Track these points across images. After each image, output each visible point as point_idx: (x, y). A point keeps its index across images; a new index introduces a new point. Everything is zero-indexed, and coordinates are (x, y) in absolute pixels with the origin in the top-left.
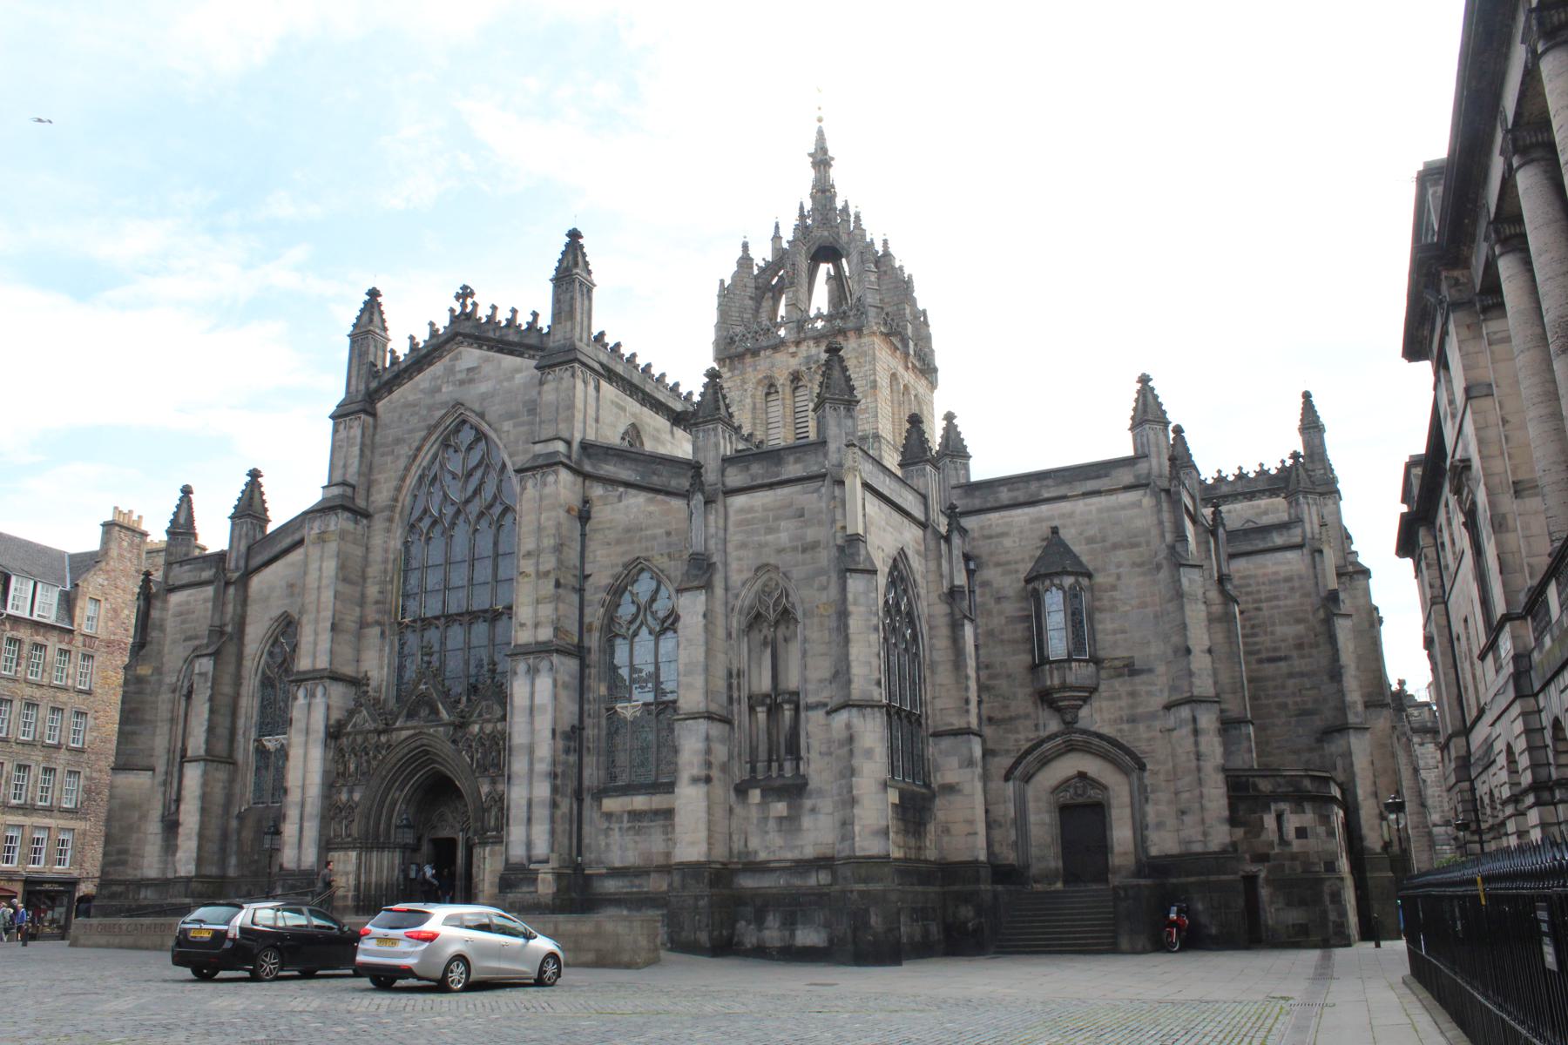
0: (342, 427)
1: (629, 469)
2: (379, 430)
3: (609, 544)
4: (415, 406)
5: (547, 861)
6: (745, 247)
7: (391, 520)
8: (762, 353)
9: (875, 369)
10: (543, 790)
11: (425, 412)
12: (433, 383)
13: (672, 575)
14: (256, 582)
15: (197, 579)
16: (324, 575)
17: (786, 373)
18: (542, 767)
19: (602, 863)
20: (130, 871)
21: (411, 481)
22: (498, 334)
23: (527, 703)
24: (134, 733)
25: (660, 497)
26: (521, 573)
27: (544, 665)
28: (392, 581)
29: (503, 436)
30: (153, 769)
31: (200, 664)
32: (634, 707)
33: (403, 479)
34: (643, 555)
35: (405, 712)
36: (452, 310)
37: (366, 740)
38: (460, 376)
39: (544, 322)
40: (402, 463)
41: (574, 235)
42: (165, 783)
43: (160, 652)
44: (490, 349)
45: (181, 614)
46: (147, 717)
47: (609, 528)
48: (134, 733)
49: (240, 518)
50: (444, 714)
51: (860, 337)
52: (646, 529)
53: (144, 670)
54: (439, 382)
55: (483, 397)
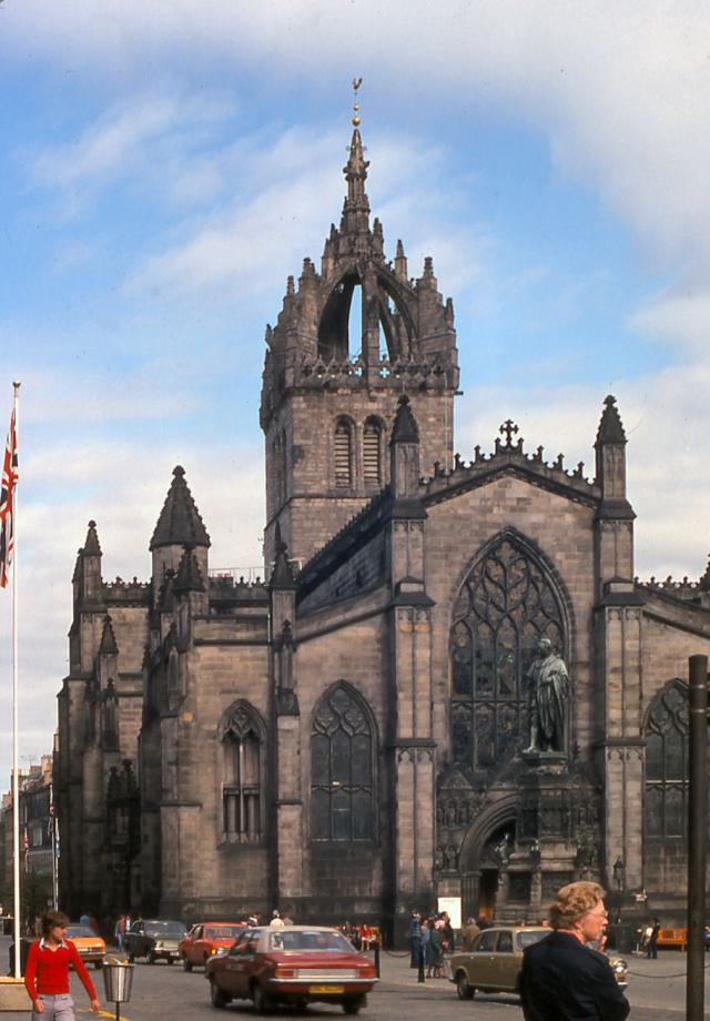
0: (401, 527)
4: (467, 519)
11: (477, 528)
14: (304, 651)
16: (419, 661)
22: (548, 475)
24: (187, 773)
29: (556, 564)
36: (498, 441)
38: (509, 503)
42: (216, 817)
43: (195, 701)
44: (539, 486)
45: (212, 668)
46: (193, 759)
48: (187, 773)
53: (188, 717)
54: (489, 503)
55: (535, 527)
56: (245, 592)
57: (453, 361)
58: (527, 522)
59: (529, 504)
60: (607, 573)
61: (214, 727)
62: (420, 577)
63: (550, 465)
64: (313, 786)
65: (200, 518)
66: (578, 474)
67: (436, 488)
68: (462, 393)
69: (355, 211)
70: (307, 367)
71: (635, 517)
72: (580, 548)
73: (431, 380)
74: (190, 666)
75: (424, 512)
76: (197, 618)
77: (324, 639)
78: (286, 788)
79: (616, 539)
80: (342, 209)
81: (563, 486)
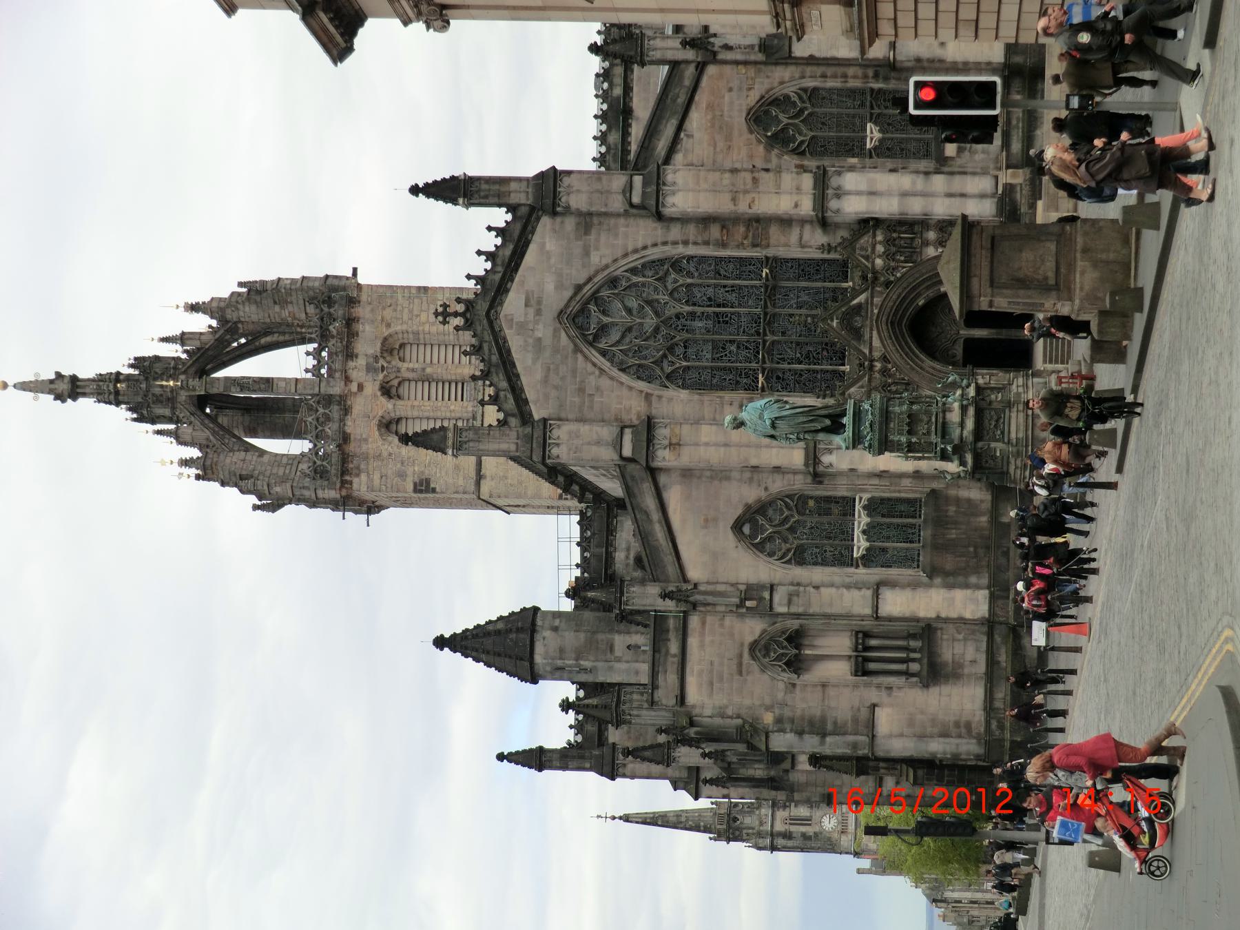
1: (666, 126)
2: (563, 415)
3: (730, 147)
4: (549, 369)
5: (996, 178)
6: (185, 463)
7: (660, 397)
8: (348, 430)
9: (403, 288)
10: (939, 182)
11: (559, 356)
12: (530, 348)
13: (767, 86)
14: (694, 573)
15: (676, 666)
17: (383, 400)
18: (920, 183)
19: (997, 158)
20: (977, 719)
21: (624, 377)
22: (500, 269)
23: (864, 198)
25: (697, 98)
26: (750, 207)
27: (834, 181)
28: (720, 397)
29: (604, 262)
30: (874, 706)
31: (780, 604)
32: (872, 133)
33: (622, 383)
34: (744, 115)
35: (853, 342)
37: (876, 389)
38: (531, 316)
39: (500, 217)
40: (605, 382)
41: (415, 190)
42: (889, 688)
44: (512, 281)
45: (711, 684)
46: (818, 713)
47: (715, 149)
48: (835, 723)
49: (622, 594)
50: (861, 298)
51: (359, 302)
52: (722, 111)
53: (768, 718)
54: (531, 341)
55: (560, 286)
56: (593, 562)
57: (317, 284)
58: (555, 297)
59: (533, 292)
60: (617, 204)
61: (781, 685)
62: (615, 430)
63: (489, 265)
64: (857, 566)
65: (501, 618)
66: (500, 232)
67: (510, 404)
68: (355, 270)
69: (117, 393)
70: (315, 471)
71: (554, 167)
72: (587, 231)
73: (338, 311)
74: (708, 712)
75: (539, 421)
76: (652, 703)
77: (681, 547)
78: (857, 603)
79: (578, 191)
80: (113, 407)
81: (514, 253)
